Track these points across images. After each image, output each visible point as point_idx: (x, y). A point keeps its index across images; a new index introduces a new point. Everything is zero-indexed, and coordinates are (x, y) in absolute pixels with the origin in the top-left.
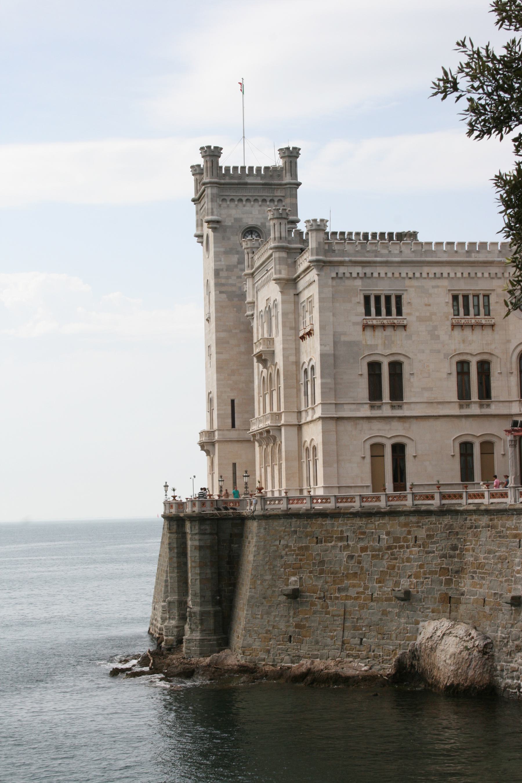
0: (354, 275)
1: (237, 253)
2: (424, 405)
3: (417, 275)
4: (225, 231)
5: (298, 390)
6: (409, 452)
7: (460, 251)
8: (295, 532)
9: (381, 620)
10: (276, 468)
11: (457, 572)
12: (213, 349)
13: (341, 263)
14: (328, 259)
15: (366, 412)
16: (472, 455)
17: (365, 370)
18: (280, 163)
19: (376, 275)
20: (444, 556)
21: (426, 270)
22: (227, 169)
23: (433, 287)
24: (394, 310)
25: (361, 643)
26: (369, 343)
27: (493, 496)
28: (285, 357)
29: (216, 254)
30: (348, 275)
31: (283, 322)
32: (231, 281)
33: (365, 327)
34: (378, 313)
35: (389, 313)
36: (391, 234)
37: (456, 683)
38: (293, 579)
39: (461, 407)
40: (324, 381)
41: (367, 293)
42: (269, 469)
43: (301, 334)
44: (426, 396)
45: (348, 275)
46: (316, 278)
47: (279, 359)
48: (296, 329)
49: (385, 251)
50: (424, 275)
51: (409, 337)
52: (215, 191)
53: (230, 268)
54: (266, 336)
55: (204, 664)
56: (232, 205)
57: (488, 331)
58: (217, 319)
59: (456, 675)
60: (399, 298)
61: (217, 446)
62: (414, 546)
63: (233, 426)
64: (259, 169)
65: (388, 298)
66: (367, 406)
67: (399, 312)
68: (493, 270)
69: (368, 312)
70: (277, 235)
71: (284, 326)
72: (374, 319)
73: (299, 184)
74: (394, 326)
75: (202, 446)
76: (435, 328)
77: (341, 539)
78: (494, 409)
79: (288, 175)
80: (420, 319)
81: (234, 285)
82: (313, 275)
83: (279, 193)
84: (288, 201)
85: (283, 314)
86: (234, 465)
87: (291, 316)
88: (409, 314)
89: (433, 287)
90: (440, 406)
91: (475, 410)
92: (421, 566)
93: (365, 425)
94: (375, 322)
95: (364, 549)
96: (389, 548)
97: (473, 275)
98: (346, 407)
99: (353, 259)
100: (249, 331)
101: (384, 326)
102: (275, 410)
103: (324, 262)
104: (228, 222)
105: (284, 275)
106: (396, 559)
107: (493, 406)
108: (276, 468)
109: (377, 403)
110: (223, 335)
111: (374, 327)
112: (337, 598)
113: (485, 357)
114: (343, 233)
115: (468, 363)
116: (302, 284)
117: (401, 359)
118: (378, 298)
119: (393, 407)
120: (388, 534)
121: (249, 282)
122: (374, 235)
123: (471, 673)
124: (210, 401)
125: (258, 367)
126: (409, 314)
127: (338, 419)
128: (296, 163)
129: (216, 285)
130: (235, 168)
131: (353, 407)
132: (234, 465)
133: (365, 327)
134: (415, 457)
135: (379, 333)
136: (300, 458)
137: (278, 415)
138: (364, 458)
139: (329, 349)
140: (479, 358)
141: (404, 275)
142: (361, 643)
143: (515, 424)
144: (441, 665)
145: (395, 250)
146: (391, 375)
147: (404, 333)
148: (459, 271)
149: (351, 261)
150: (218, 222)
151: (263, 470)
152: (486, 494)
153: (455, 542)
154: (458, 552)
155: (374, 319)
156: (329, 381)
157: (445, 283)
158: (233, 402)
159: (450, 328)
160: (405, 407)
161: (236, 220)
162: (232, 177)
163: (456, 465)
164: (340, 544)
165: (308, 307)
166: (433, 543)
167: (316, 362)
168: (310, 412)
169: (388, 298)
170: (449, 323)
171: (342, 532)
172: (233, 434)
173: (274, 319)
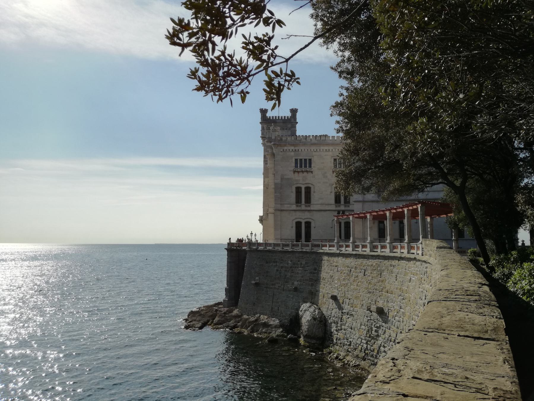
0: (291, 150)
2: (319, 205)
3: (318, 150)
6: (313, 225)
8: (259, 258)
9: (286, 299)
11: (316, 281)
17: (294, 190)
18: (289, 114)
19: (300, 150)
20: (311, 273)
21: (322, 148)
22: (270, 117)
23: (325, 155)
26: (296, 179)
30: (288, 150)
33: (294, 172)
35: (306, 167)
38: (257, 278)
39: (336, 206)
40: (276, 194)
41: (296, 158)
44: (321, 201)
45: (288, 150)
50: (321, 150)
60: (310, 160)
62: (300, 267)
65: (305, 160)
66: (294, 206)
67: (310, 166)
69: (296, 166)
70: (268, 136)
73: (297, 123)
74: (307, 172)
77: (275, 262)
88: (314, 167)
89: (325, 155)
92: (302, 277)
95: (282, 267)
96: (291, 267)
98: (285, 205)
101: (303, 172)
103: (278, 145)
106: (293, 272)
107: (351, 206)
109: (299, 205)
112: (271, 288)
117: (310, 186)
119: (306, 206)
120: (291, 261)
123: (314, 330)
126: (314, 167)
127: (282, 210)
128: (296, 115)
130: (273, 117)
131: (289, 206)
133: (294, 172)
134: (315, 227)
135: (301, 174)
138: (292, 227)
139: (278, 181)
141: (312, 150)
143: (339, 213)
146: (305, 192)
147: (312, 175)
153: (316, 267)
154: (316, 271)
157: (330, 153)
160: (312, 206)
164: (274, 264)
166: (307, 266)
170: (331, 171)
171: (275, 259)
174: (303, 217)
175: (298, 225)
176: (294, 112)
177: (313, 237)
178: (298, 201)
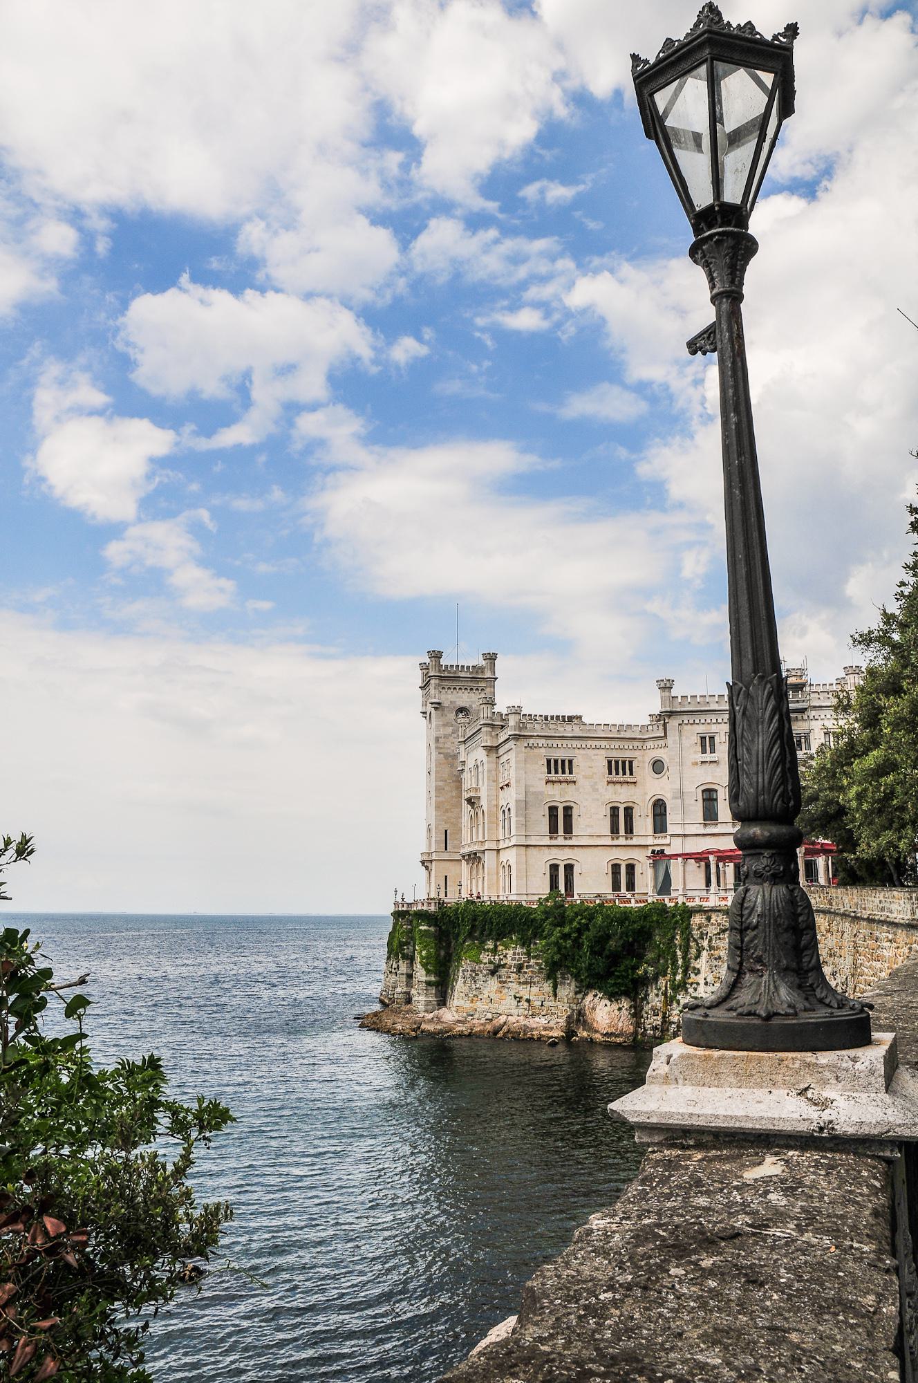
1: (452, 725)
4: (443, 710)
5: (498, 825)
6: (576, 870)
7: (612, 729)
10: (480, 880)
12: (433, 793)
13: (531, 737)
14: (522, 734)
15: (547, 841)
16: (620, 873)
21: (589, 743)
22: (446, 666)
23: (595, 755)
24: (567, 769)
25: (542, 1005)
27: (637, 902)
28: (489, 801)
29: (437, 726)
31: (488, 777)
32: (446, 746)
33: (547, 782)
34: (556, 772)
35: (564, 772)
36: (563, 717)
37: (610, 1032)
39: (613, 839)
42: (474, 881)
43: (501, 786)
46: (514, 746)
47: (484, 802)
48: (496, 781)
49: (563, 729)
51: (577, 790)
52: (437, 681)
53: (446, 737)
54: (474, 786)
55: (429, 1017)
56: (449, 691)
57: (633, 785)
58: (437, 772)
59: (610, 1027)
60: (570, 762)
61: (434, 863)
63: (446, 849)
64: (468, 667)
67: (571, 773)
68: (636, 744)
69: (549, 772)
70: (485, 715)
71: (488, 779)
72: (553, 777)
74: (567, 782)
75: (423, 863)
76: (596, 783)
78: (635, 841)
79: (489, 672)
80: (585, 777)
81: (449, 748)
82: (511, 744)
83: (482, 684)
84: (488, 690)
85: (489, 771)
86: (446, 877)
87: (494, 773)
88: (577, 773)
89: (595, 755)
90: (599, 838)
91: (622, 841)
93: (546, 849)
94: (554, 779)
97: (621, 747)
99: (540, 734)
100: (458, 782)
101: (560, 782)
102: (480, 839)
103: (519, 735)
104: (446, 704)
105: (489, 744)
107: (635, 839)
108: (480, 880)
110: (440, 783)
111: (553, 782)
112: (526, 973)
113: (630, 805)
114: (530, 715)
115: (617, 808)
116: (501, 751)
117: (572, 804)
118: (556, 761)
119: (565, 838)
121: (462, 747)
122: (552, 717)
123: (620, 1024)
124: (430, 830)
125: (466, 808)
126: (577, 773)
127: (527, 846)
129: (437, 748)
130: (452, 666)
132: (446, 877)
133: (547, 782)
135: (557, 786)
136: (498, 873)
137: (483, 842)
139: (522, 797)
140: (625, 805)
142: (542, 1005)
143: (653, 852)
144: (599, 1019)
145: (569, 728)
148: (613, 743)
149: (538, 736)
150: (439, 704)
151: (469, 881)
152: (633, 901)
155: (553, 777)
156: (521, 819)
157: (603, 752)
158: (446, 831)
159: (606, 783)
160: (574, 838)
161: (451, 702)
162: (449, 672)
163: (609, 880)
165: (506, 766)
167: (512, 806)
168: (507, 840)
169: (563, 762)
172: (446, 856)
173: (480, 775)
174: (561, 857)
175: (554, 868)
176: (491, 658)
177: (577, 890)
178: (553, 829)
